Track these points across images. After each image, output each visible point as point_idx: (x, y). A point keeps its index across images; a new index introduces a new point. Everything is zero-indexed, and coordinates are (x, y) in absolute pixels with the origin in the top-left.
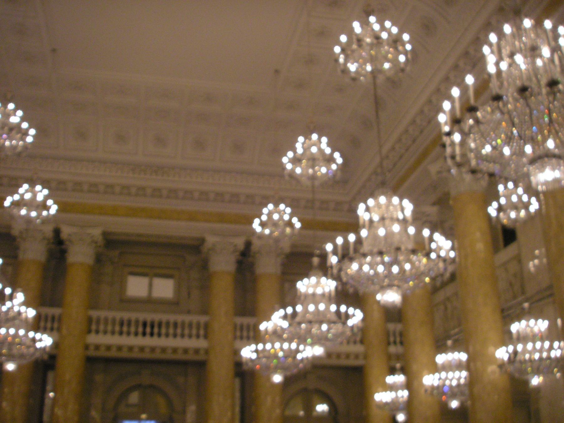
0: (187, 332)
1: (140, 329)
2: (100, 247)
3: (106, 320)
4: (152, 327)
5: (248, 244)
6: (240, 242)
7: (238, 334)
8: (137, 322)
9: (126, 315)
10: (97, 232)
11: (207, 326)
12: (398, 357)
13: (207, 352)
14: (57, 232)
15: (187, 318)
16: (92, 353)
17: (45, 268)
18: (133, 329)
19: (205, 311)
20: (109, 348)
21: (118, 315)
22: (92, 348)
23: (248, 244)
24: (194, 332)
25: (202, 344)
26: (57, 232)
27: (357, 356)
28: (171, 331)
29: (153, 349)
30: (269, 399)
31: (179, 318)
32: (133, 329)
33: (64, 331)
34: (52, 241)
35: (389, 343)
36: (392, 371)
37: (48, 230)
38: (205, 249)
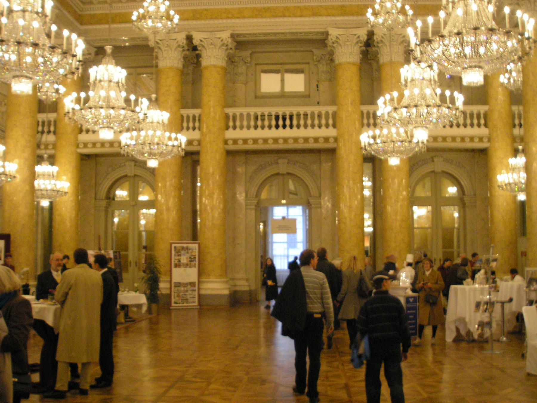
0: (316, 122)
1: (274, 123)
2: (231, 49)
3: (241, 115)
4: (284, 119)
5: (371, 34)
6: (363, 34)
7: (365, 121)
8: (270, 115)
9: (259, 111)
10: (225, 35)
11: (335, 114)
12: (522, 140)
13: (336, 140)
14: (189, 38)
15: (316, 109)
16: (231, 147)
17: (183, 73)
18: (266, 123)
19: (334, 101)
20: (245, 141)
21: (252, 111)
22: (230, 142)
23: (371, 34)
24: (323, 122)
25: (331, 132)
26: (189, 38)
27: (481, 139)
28: (302, 122)
29: (286, 140)
30: (396, 181)
31: (309, 110)
32: (266, 123)
33: (205, 130)
34: (186, 48)
35: (514, 126)
36: (516, 153)
37: (181, 38)
38: (329, 42)
